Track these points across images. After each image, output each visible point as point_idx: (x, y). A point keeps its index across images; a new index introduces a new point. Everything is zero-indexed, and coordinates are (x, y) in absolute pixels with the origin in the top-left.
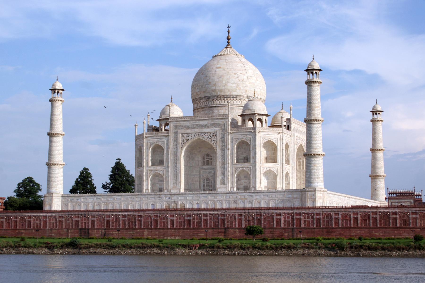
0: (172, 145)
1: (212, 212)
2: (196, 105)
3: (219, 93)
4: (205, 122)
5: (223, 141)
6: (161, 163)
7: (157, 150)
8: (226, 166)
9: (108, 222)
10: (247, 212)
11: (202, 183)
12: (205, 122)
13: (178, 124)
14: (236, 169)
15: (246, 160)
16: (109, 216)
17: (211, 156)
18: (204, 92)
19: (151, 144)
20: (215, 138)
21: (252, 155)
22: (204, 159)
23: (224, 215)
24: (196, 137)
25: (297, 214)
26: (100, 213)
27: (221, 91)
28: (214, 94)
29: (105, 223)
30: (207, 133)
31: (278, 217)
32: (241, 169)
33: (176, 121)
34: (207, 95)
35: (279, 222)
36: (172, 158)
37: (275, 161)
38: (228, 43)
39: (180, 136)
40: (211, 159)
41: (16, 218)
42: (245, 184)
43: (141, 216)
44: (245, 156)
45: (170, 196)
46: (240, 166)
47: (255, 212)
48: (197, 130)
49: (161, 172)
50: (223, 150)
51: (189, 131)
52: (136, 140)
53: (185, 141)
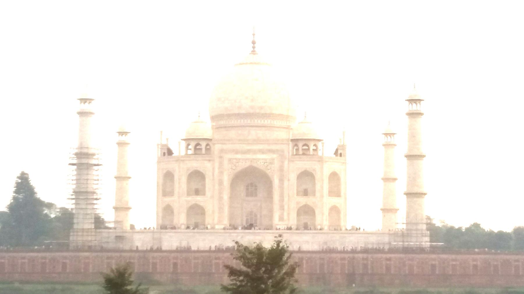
0: (217, 171)
1: (309, 255)
2: (222, 123)
3: (258, 111)
4: (261, 147)
5: (281, 169)
6: (197, 192)
7: (197, 176)
8: (286, 199)
9: (175, 264)
10: (351, 255)
11: (245, 219)
12: (261, 147)
13: (225, 147)
14: (298, 203)
15: (306, 193)
16: (176, 258)
17: (256, 186)
18: (239, 108)
19: (188, 170)
20: (273, 166)
21: (318, 187)
22: (247, 189)
23: (323, 259)
24: (248, 164)
25: (409, 260)
26: (165, 254)
27: (261, 108)
28: (252, 111)
29: (172, 266)
30: (263, 159)
31: (388, 262)
32: (304, 203)
33: (222, 144)
34: (243, 111)
35: (388, 268)
36: (217, 187)
37: (338, 195)
38: (254, 47)
39: (226, 162)
40: (256, 189)
41: (45, 258)
42: (305, 221)
43: (218, 258)
44: (304, 187)
45: (243, 234)
46: (303, 200)
47: (361, 255)
48: (248, 156)
49: (202, 204)
50: (281, 180)
51: (239, 156)
52: (159, 162)
53: (234, 168)
